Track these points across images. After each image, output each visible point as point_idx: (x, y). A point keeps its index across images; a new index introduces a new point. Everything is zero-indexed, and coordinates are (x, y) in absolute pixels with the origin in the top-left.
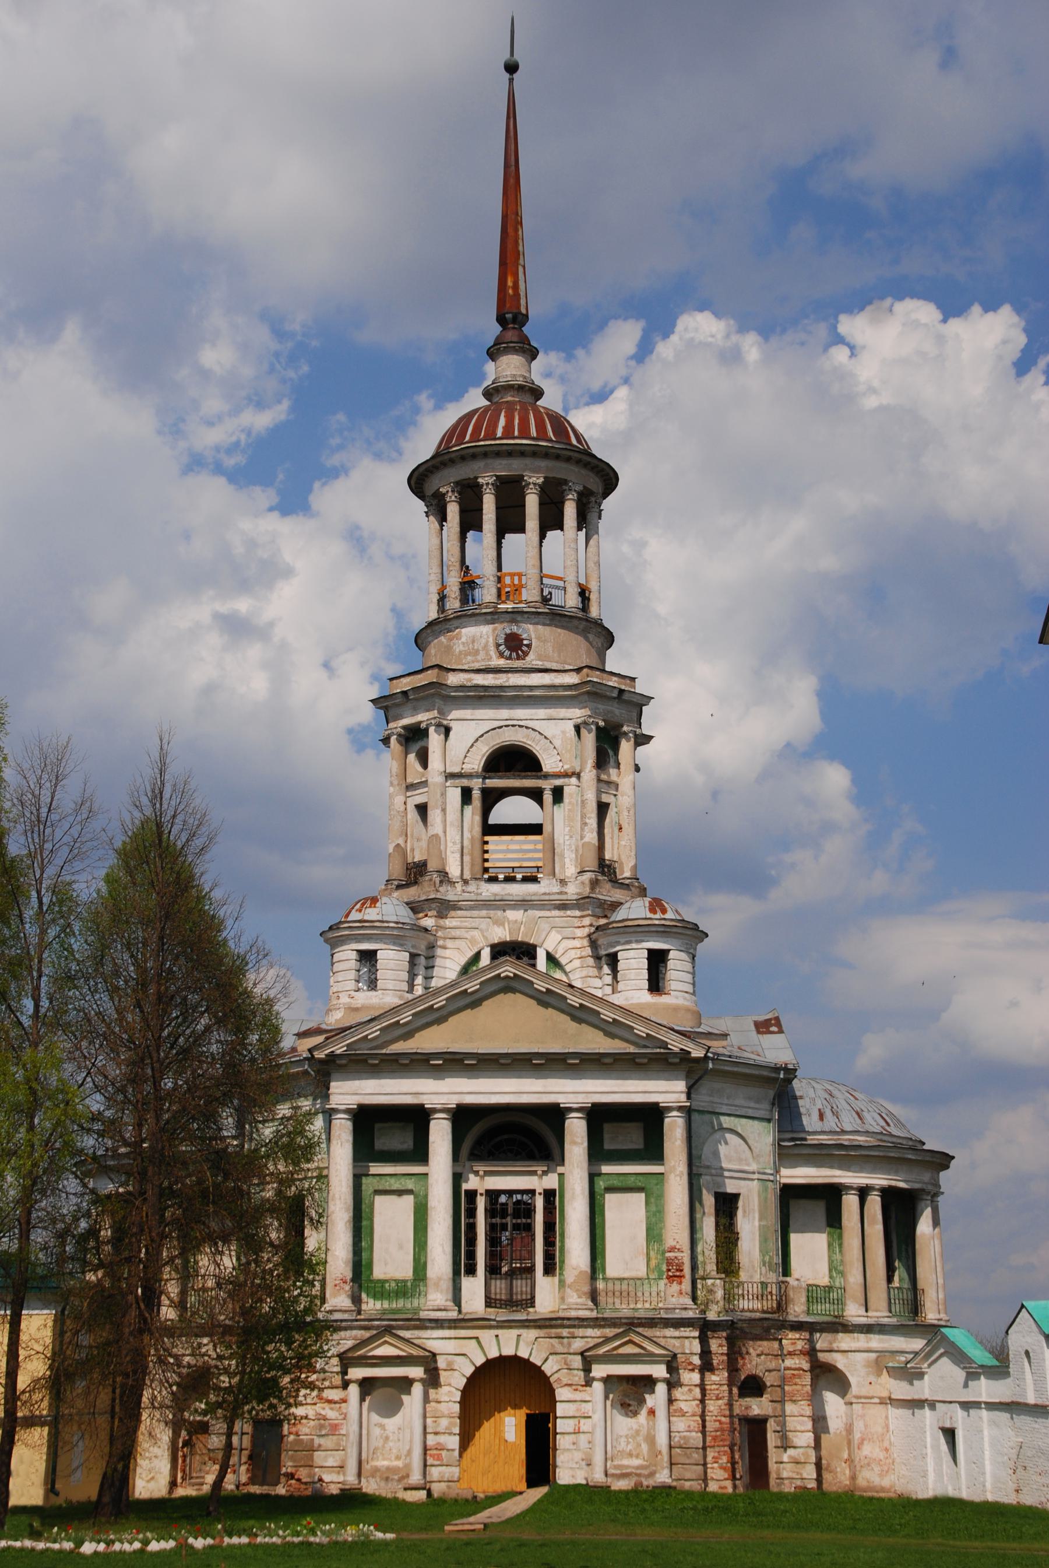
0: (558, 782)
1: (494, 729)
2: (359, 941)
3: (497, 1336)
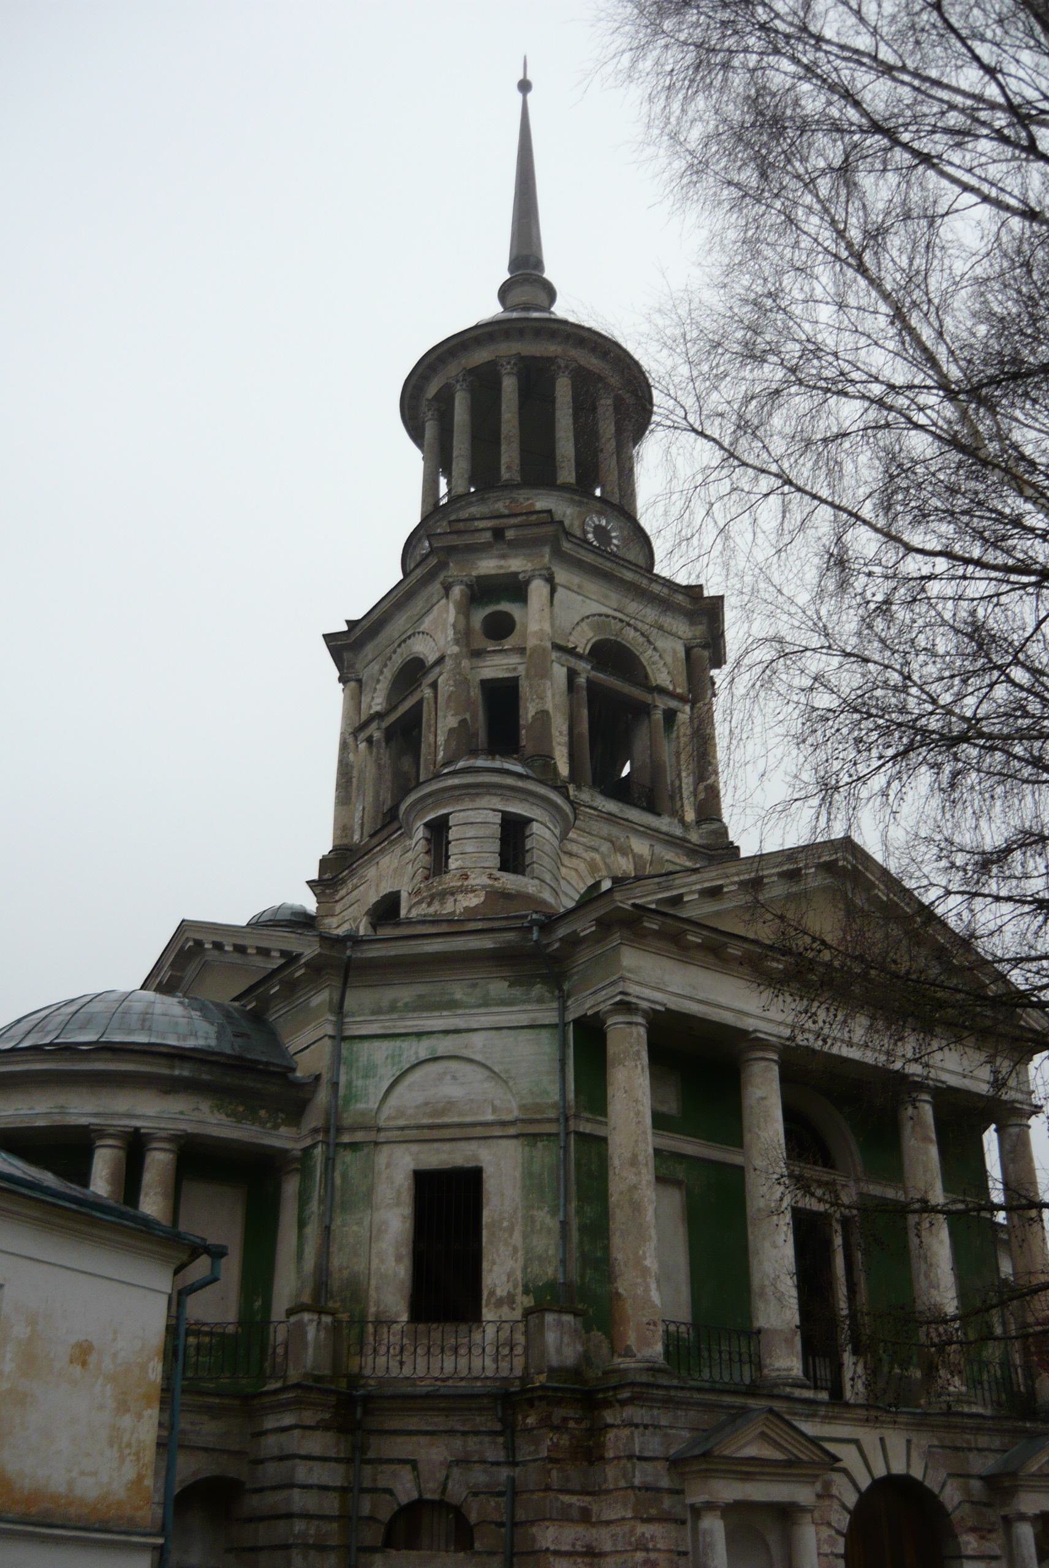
0: (673, 704)
1: (600, 615)
2: (506, 798)
3: (882, 1440)
